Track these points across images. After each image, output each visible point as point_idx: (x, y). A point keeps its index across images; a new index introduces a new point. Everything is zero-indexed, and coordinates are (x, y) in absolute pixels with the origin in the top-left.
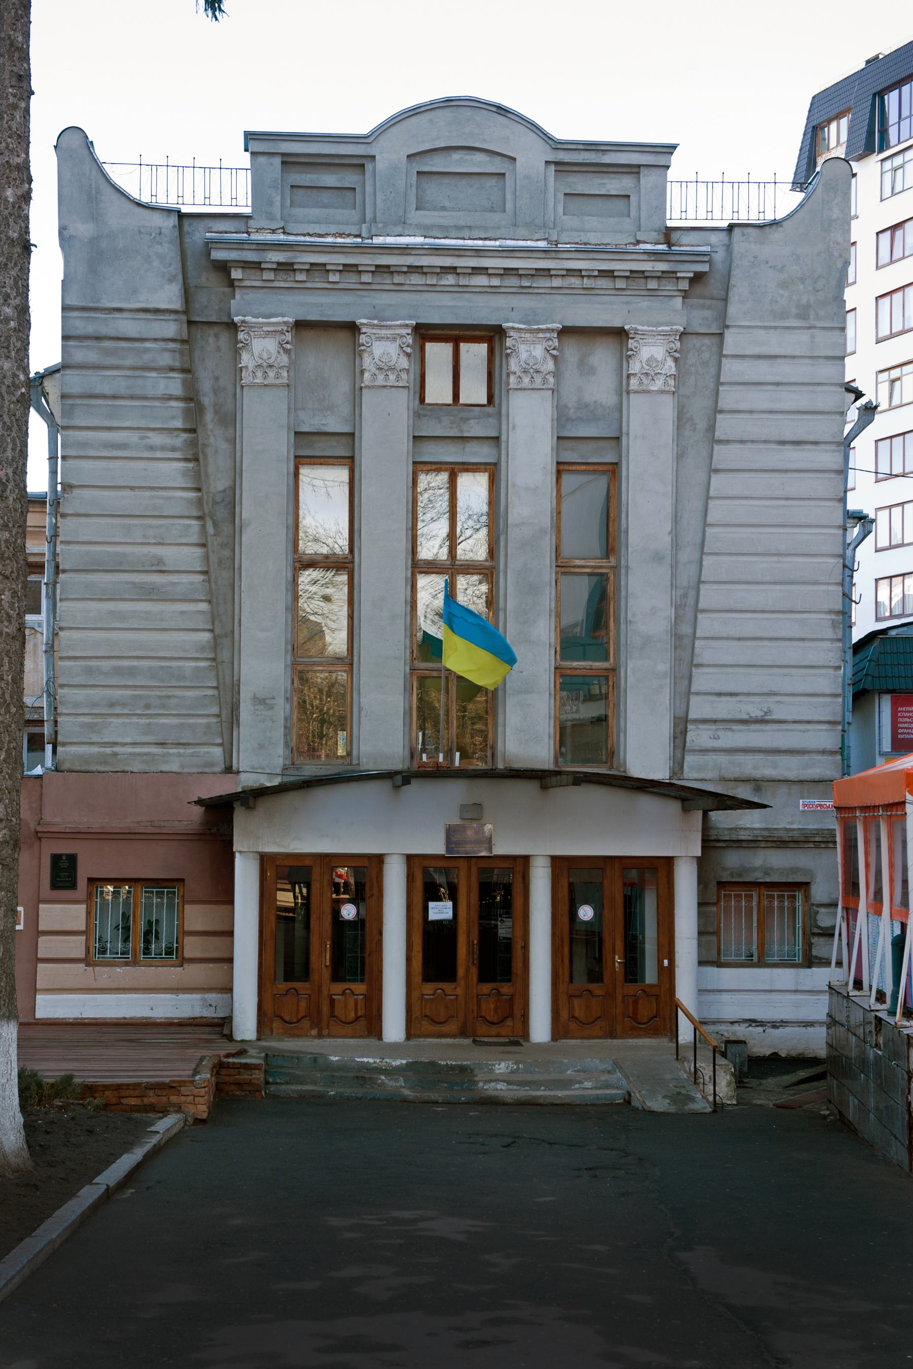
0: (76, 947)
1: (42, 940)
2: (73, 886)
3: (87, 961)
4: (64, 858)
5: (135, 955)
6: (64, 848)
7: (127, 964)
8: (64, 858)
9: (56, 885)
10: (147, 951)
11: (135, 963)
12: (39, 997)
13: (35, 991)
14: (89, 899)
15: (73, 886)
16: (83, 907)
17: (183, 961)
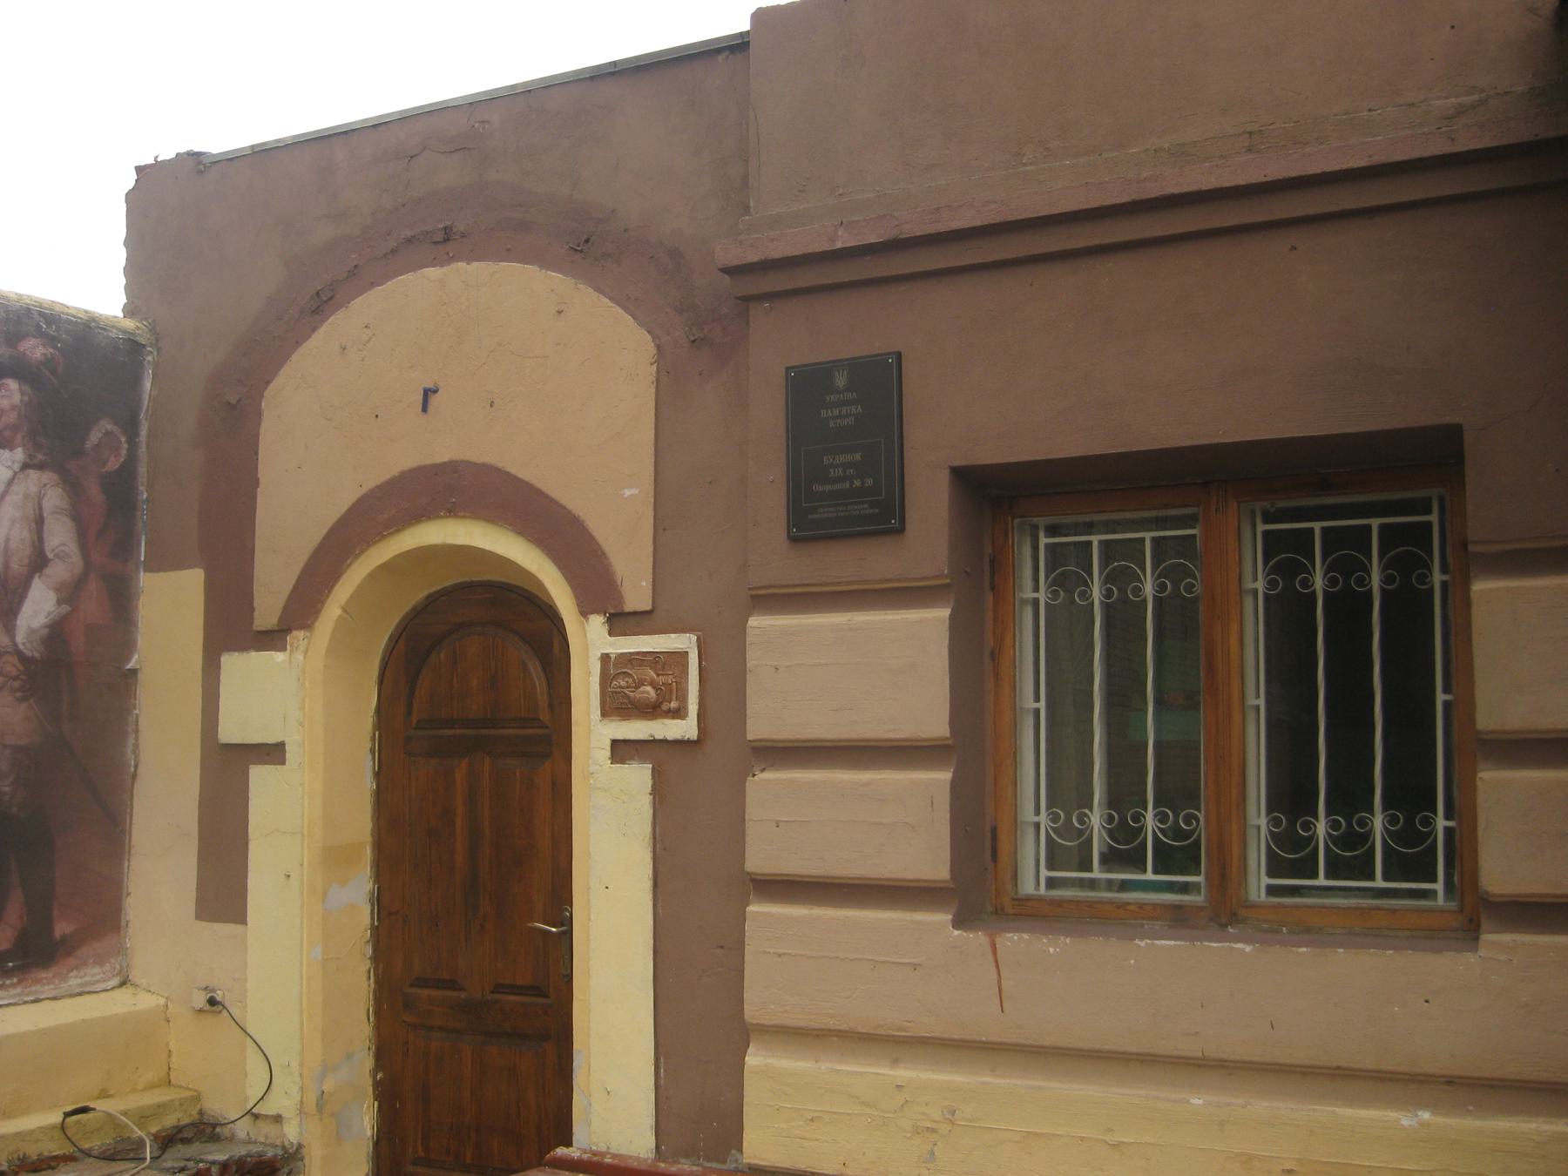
0: (905, 820)
1: (766, 782)
2: (883, 516)
3: (976, 889)
4: (841, 380)
5: (1226, 880)
6: (842, 333)
7: (1179, 920)
8: (841, 380)
9: (811, 521)
10: (1291, 857)
11: (1226, 913)
12: (754, 1059)
13: (742, 1034)
14: (978, 592)
15: (883, 516)
16: (941, 614)
17: (1476, 914)
